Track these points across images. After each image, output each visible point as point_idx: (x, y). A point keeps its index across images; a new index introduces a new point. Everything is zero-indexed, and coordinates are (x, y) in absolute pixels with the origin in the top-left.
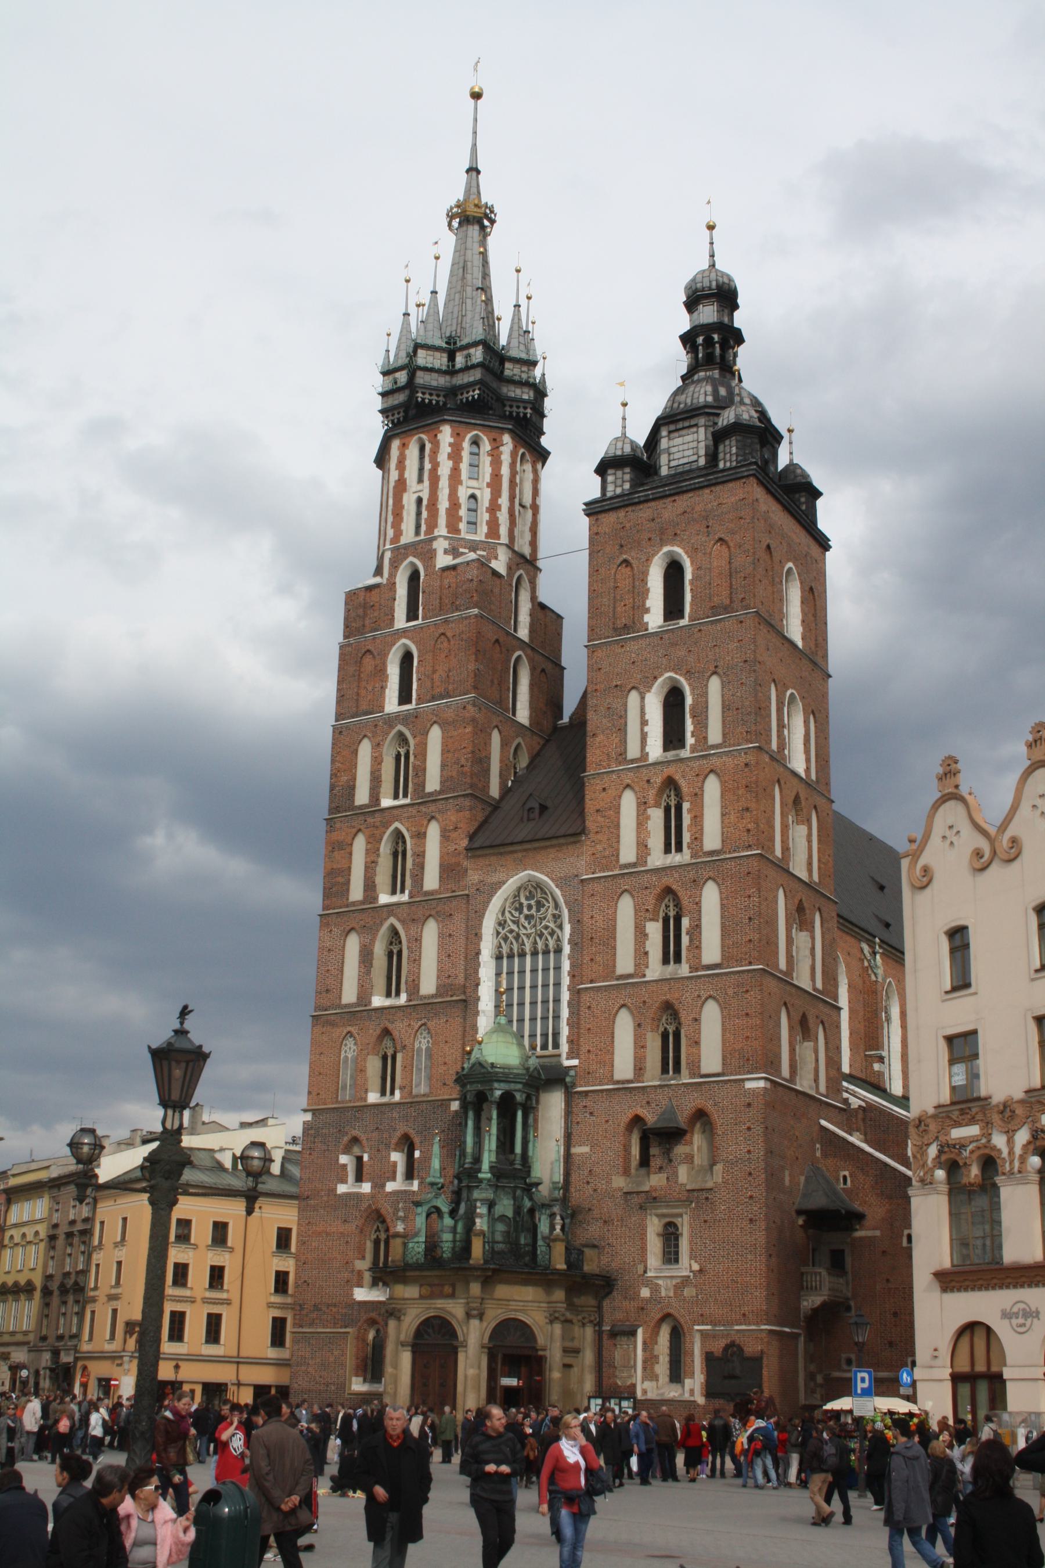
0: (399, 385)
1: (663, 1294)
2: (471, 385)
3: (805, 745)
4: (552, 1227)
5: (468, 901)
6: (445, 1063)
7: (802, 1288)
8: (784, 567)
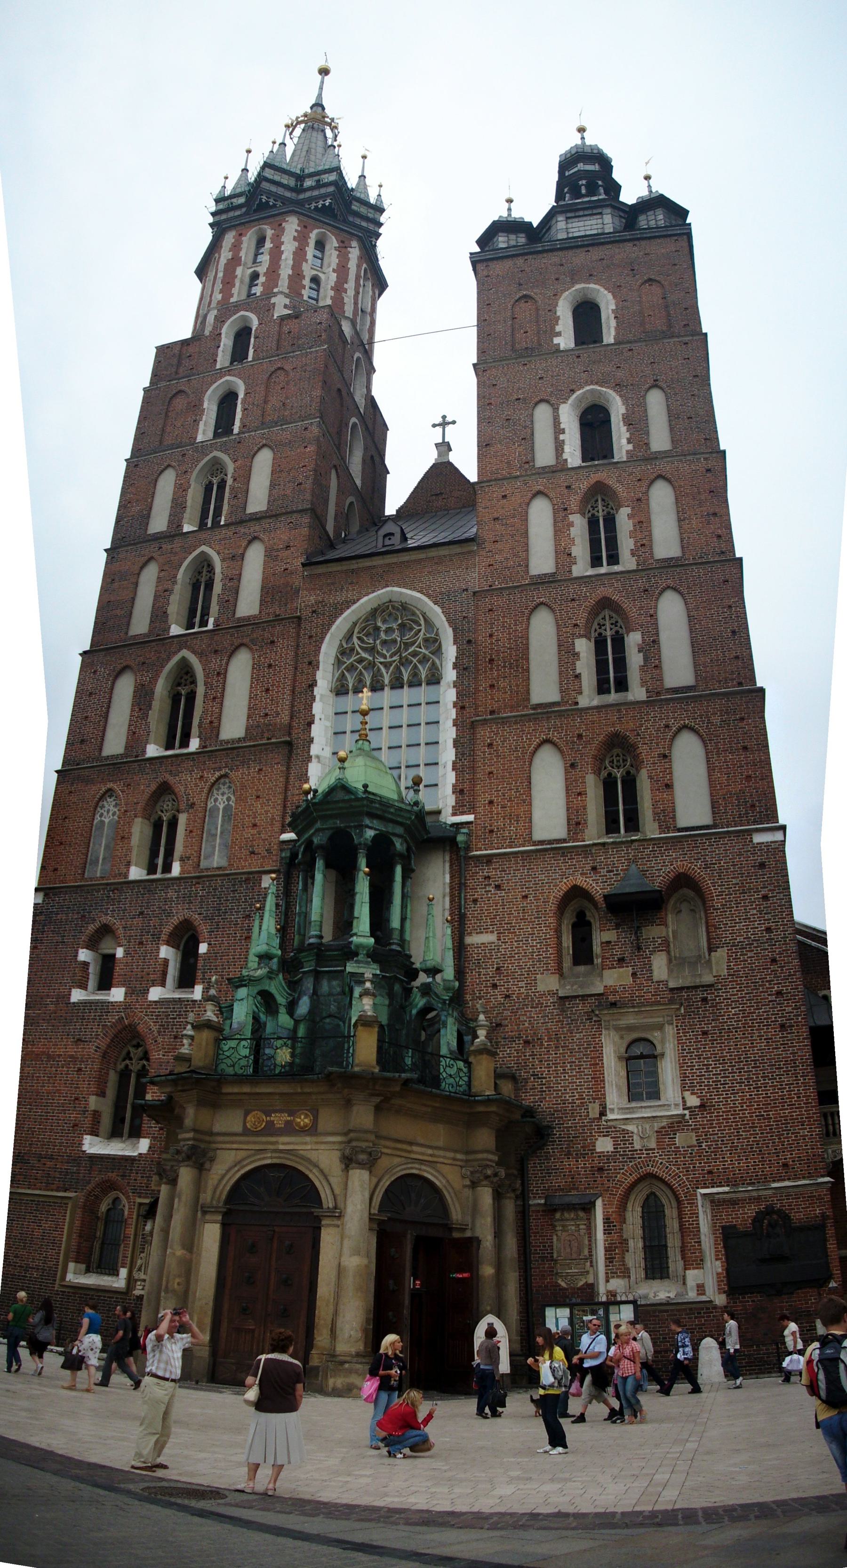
1: (637, 1146)
2: (324, 197)
5: (299, 625)
6: (255, 825)
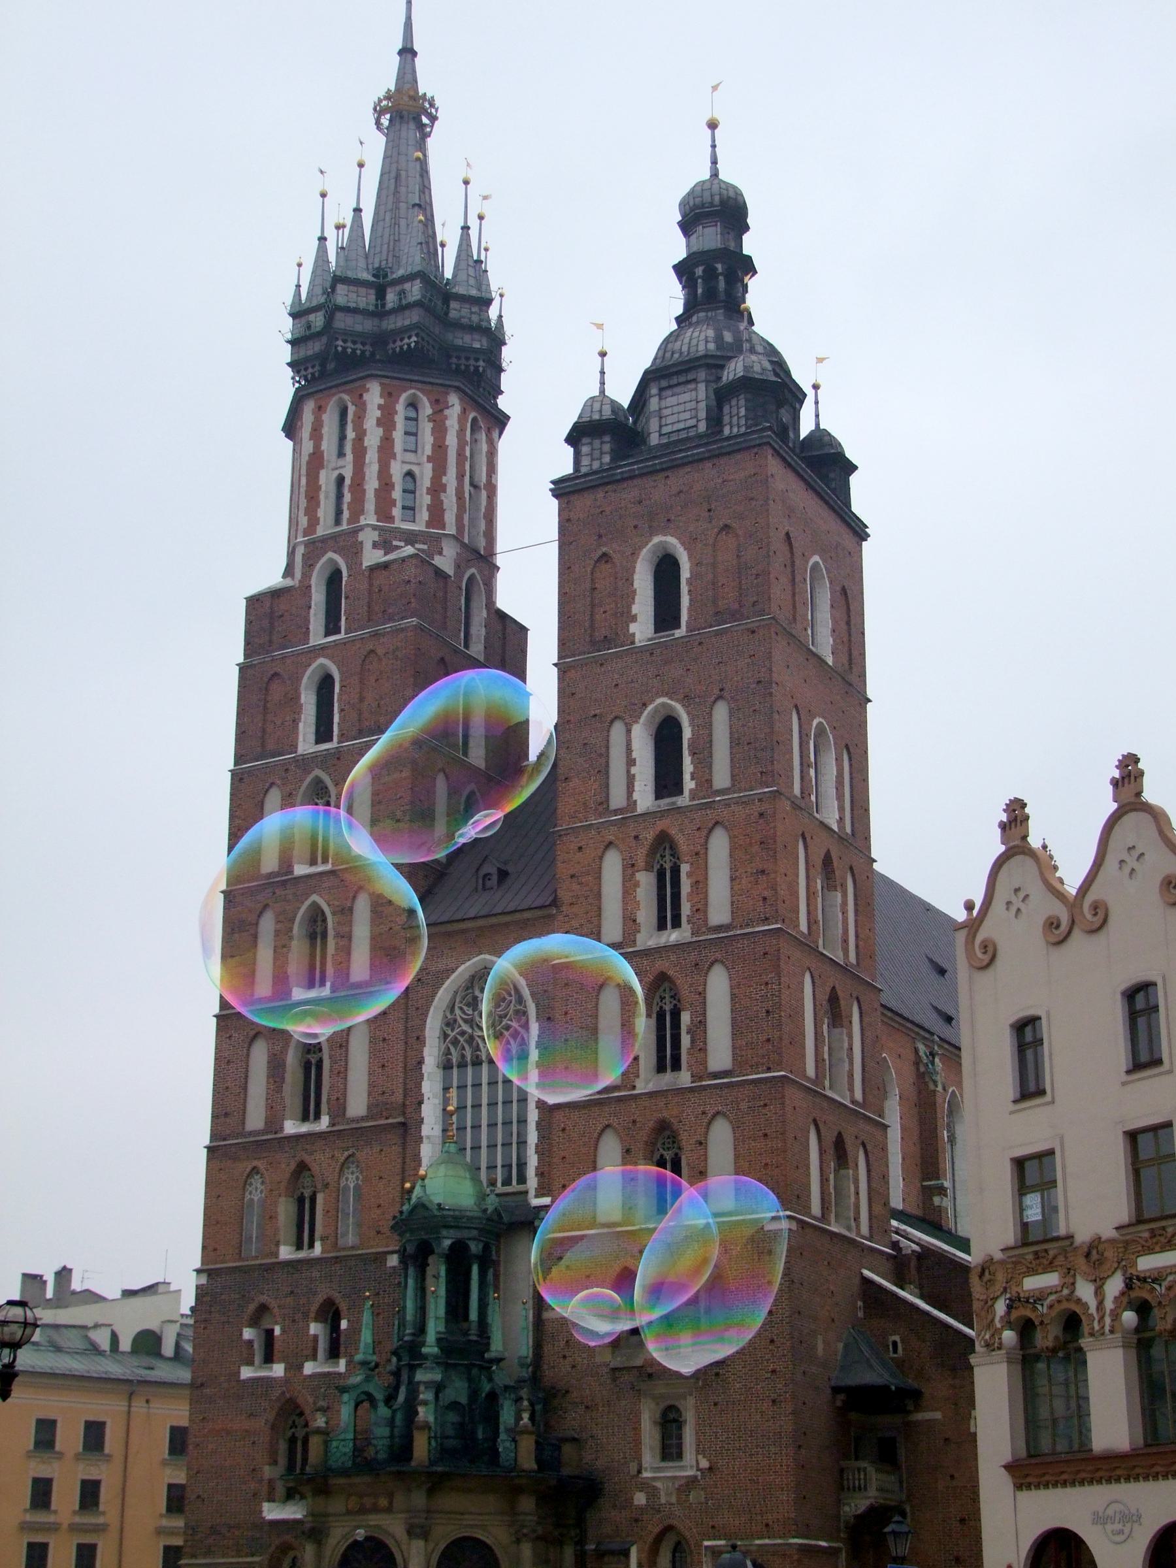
0: (313, 330)
1: (663, 1501)
3: (837, 789)
4: (519, 1418)
7: (843, 1489)
8: (807, 562)
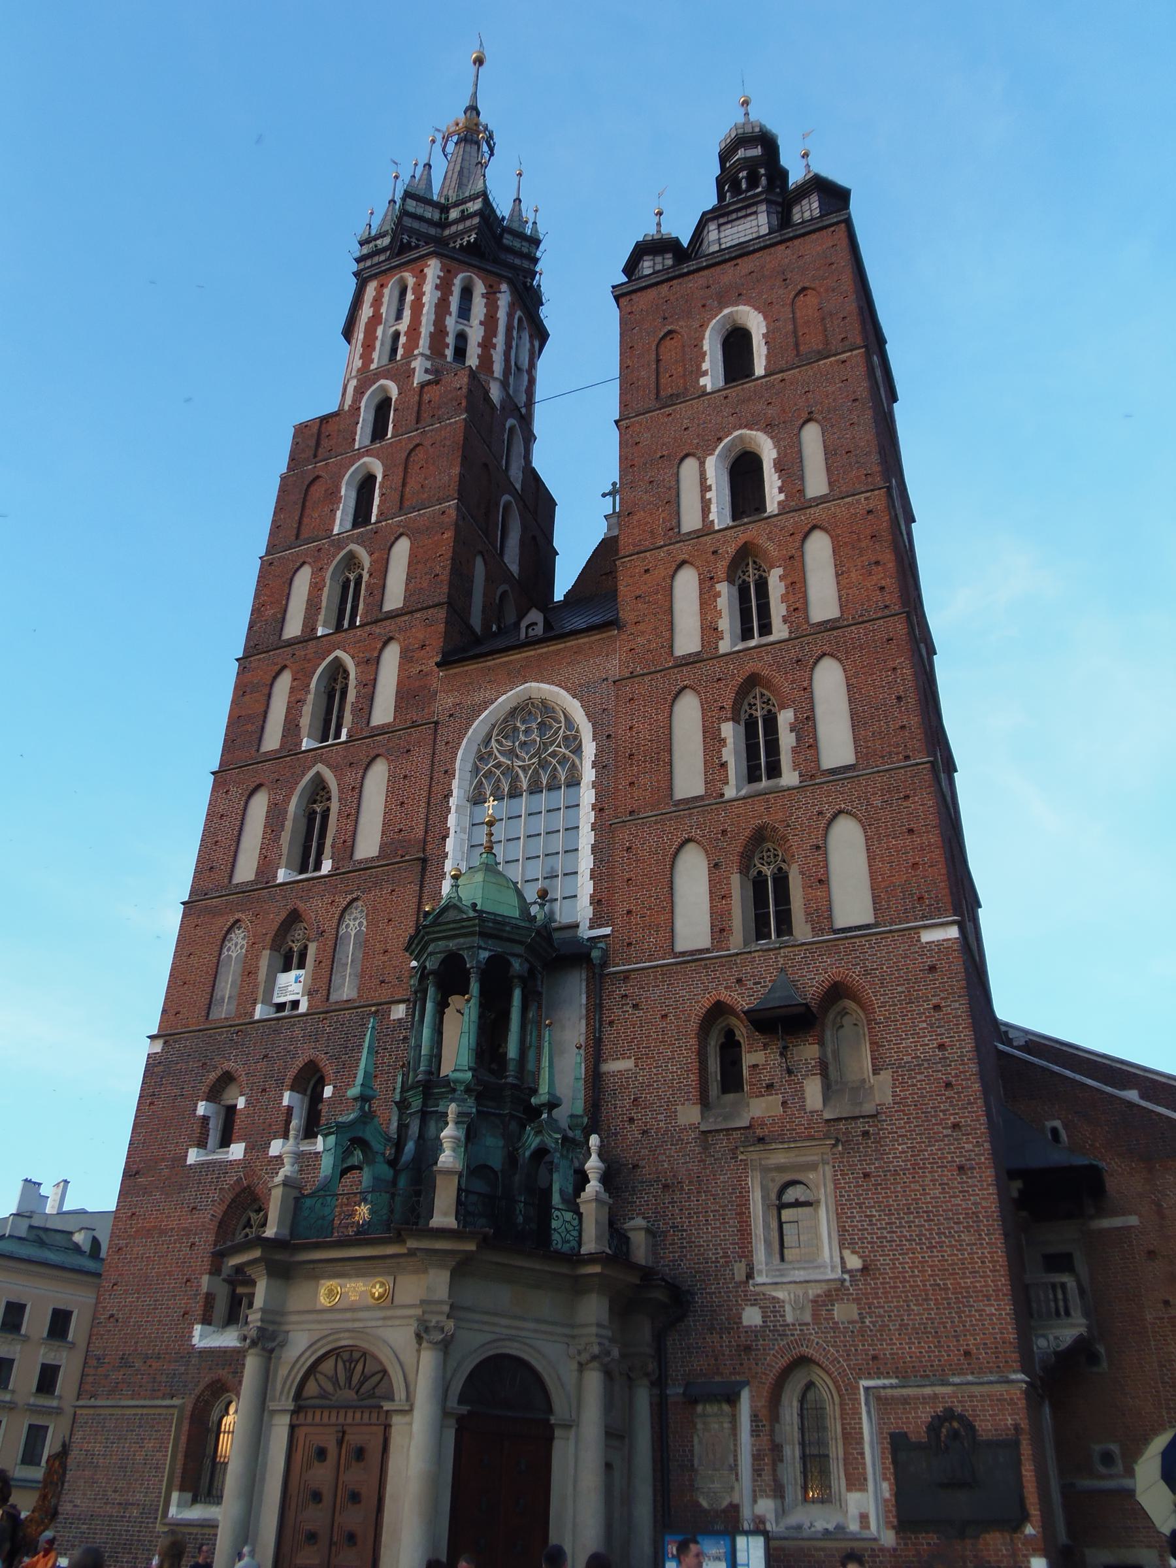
1: (789, 1319)
2: (467, 231)
5: (436, 730)
